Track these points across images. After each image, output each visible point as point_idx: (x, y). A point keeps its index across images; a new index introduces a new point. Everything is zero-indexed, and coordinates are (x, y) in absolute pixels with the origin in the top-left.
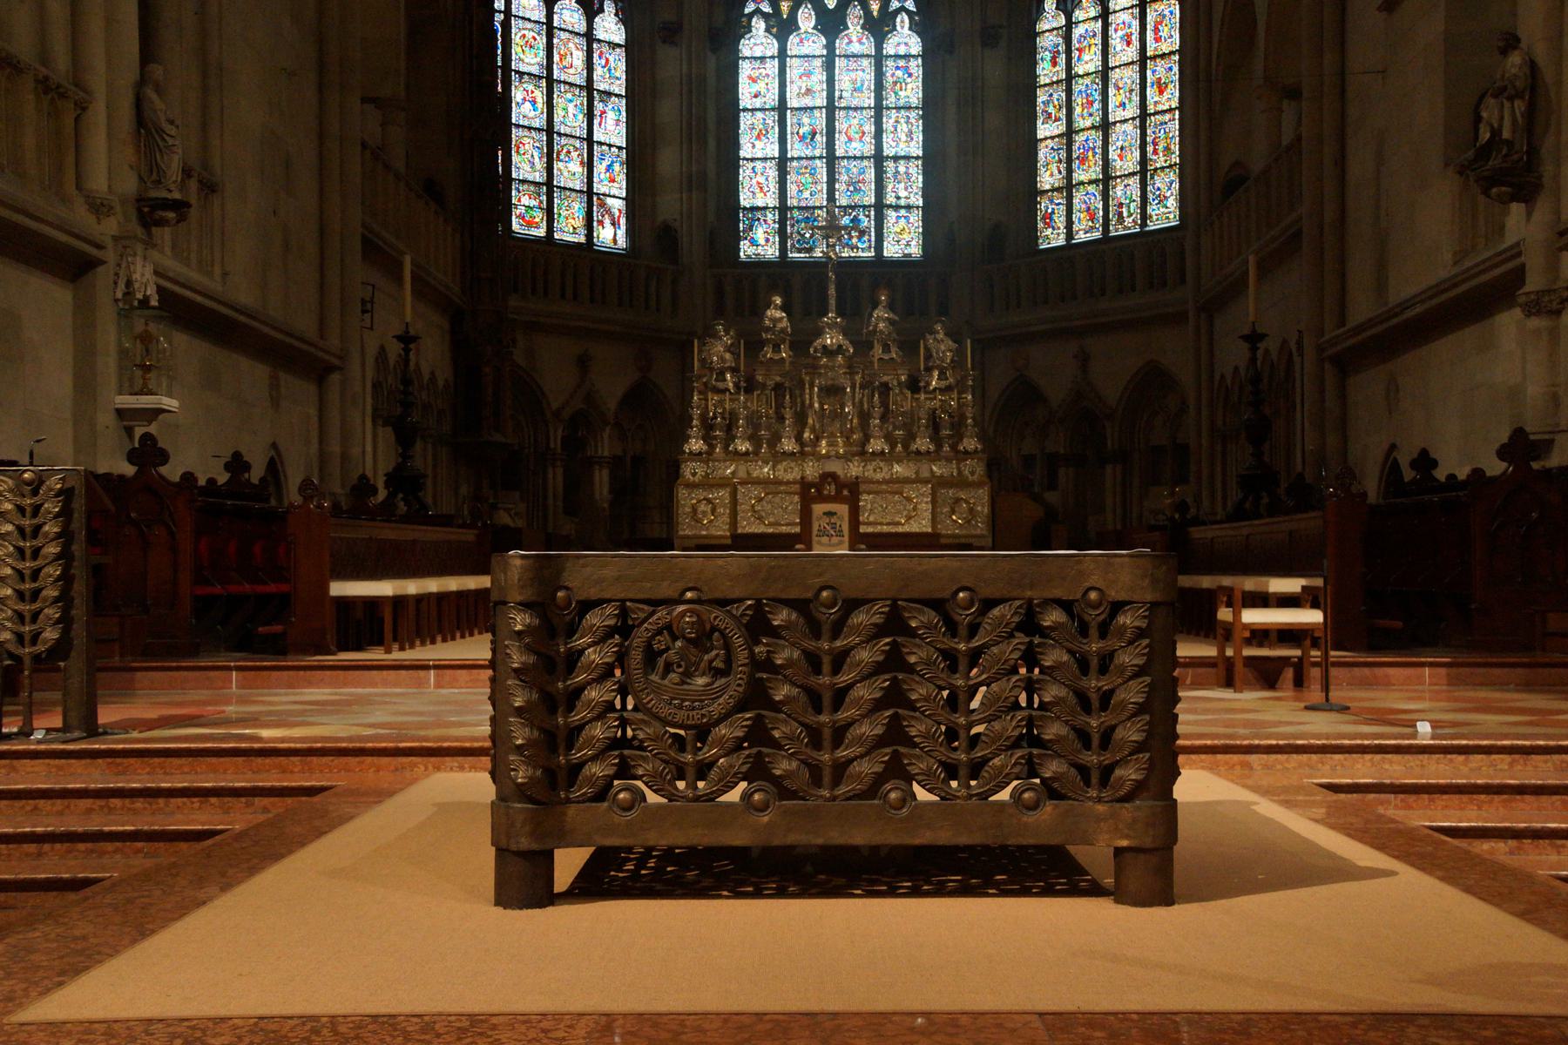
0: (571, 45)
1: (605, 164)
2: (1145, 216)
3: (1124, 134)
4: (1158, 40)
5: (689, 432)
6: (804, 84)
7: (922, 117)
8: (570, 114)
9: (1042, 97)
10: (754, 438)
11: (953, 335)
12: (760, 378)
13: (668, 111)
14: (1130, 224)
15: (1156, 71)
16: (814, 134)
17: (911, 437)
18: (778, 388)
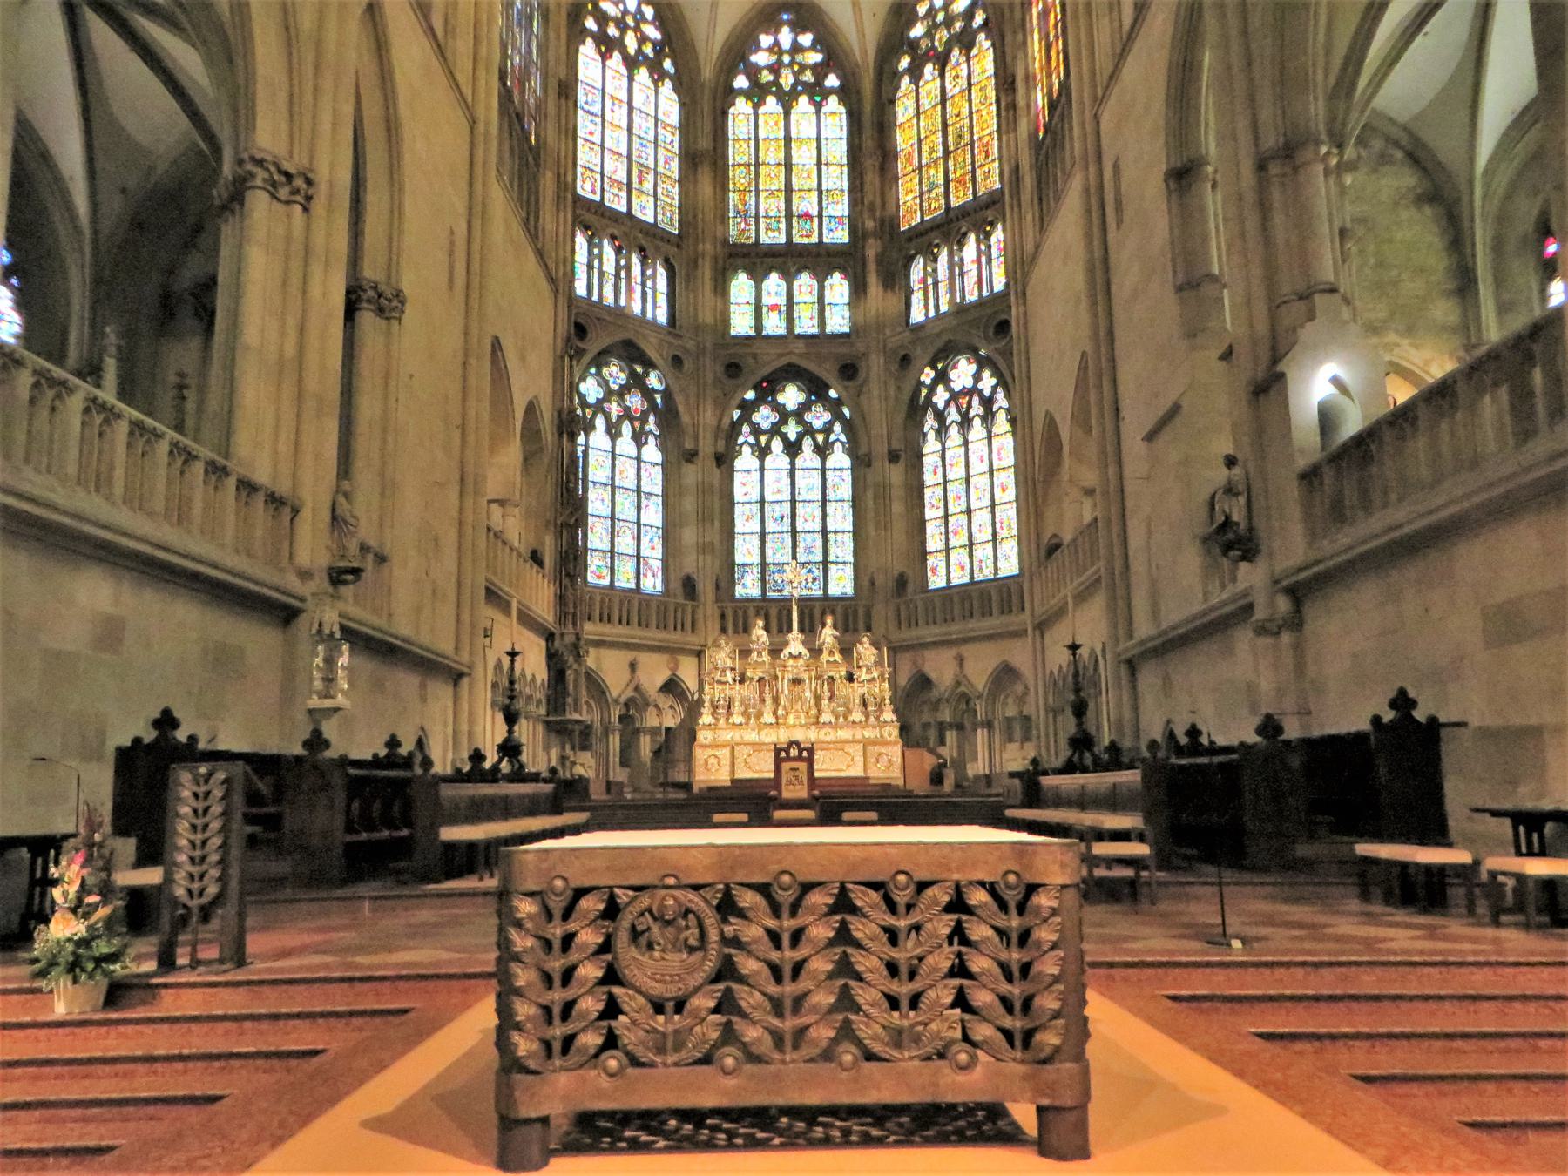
0: (627, 465)
1: (649, 537)
2: (996, 569)
3: (982, 518)
4: (1000, 459)
5: (702, 710)
6: (776, 486)
7: (854, 507)
9: (928, 492)
10: (745, 714)
11: (876, 645)
12: (748, 674)
14: (986, 573)
15: (999, 478)
16: (782, 517)
17: (849, 711)
18: (761, 680)
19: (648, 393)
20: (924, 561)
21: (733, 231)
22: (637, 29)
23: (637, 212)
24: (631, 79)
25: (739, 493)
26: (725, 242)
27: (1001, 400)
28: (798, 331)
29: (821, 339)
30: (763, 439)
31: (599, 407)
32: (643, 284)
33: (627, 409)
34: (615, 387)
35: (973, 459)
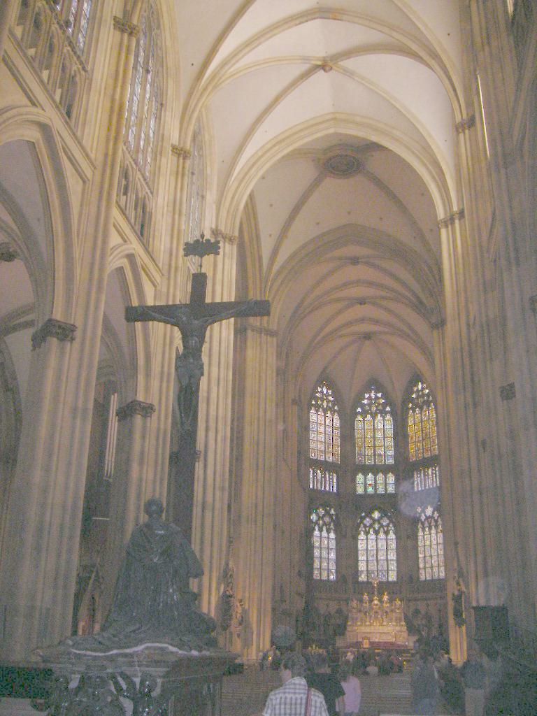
3: (435, 558)
8: (325, 554)
9: (419, 549)
14: (436, 576)
19: (331, 516)
20: (418, 571)
24: (325, 417)
25: (360, 547)
26: (354, 464)
27: (440, 521)
28: (378, 492)
29: (386, 496)
30: (367, 529)
31: (317, 523)
34: (321, 515)
35: (432, 539)
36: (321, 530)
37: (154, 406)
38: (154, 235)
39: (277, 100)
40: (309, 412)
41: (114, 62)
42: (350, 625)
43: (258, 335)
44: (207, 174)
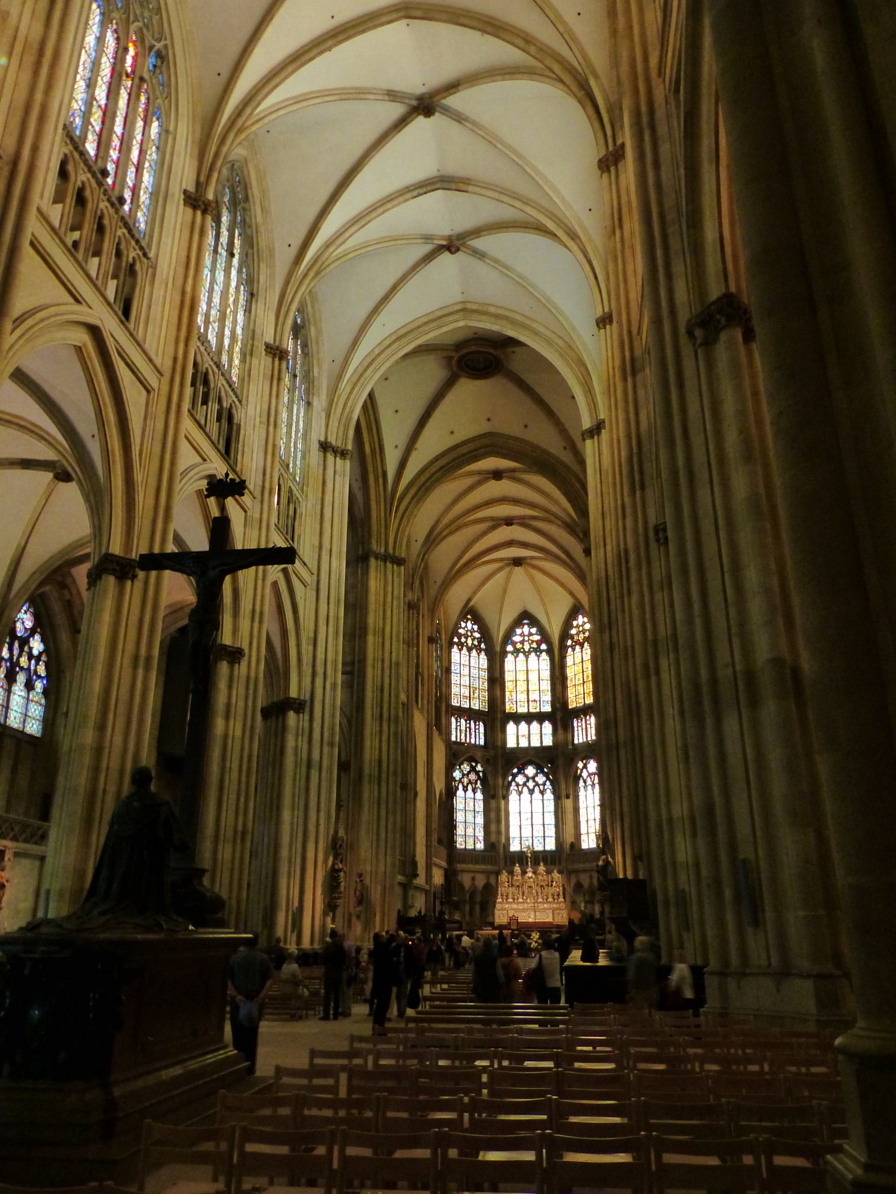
8: (470, 818)
11: (559, 872)
13: (493, 815)
18: (518, 886)
19: (477, 773)
21: (507, 707)
22: (472, 635)
23: (472, 707)
24: (470, 656)
29: (543, 749)
30: (520, 789)
31: (460, 781)
32: (475, 732)
33: (470, 780)
34: (466, 772)
36: (465, 789)
37: (243, 650)
38: (243, 451)
39: (394, 289)
40: (450, 652)
41: (185, 245)
42: (500, 903)
43: (382, 563)
44: (313, 376)
